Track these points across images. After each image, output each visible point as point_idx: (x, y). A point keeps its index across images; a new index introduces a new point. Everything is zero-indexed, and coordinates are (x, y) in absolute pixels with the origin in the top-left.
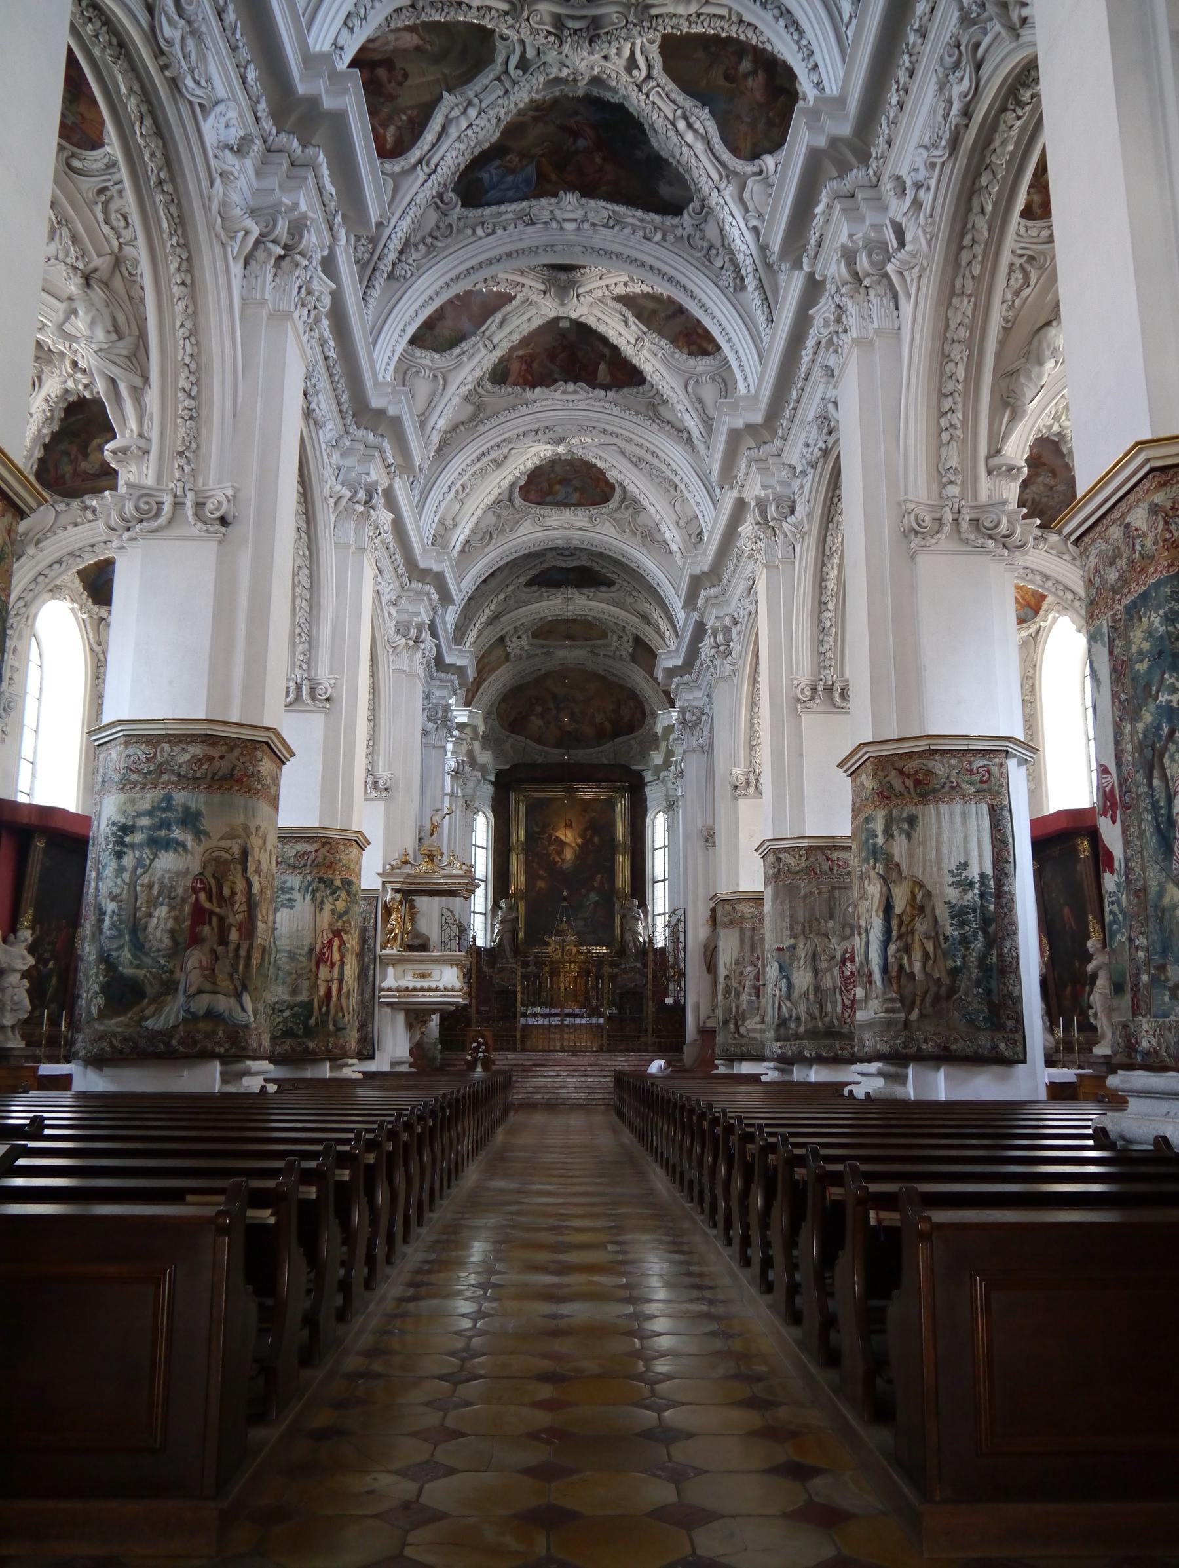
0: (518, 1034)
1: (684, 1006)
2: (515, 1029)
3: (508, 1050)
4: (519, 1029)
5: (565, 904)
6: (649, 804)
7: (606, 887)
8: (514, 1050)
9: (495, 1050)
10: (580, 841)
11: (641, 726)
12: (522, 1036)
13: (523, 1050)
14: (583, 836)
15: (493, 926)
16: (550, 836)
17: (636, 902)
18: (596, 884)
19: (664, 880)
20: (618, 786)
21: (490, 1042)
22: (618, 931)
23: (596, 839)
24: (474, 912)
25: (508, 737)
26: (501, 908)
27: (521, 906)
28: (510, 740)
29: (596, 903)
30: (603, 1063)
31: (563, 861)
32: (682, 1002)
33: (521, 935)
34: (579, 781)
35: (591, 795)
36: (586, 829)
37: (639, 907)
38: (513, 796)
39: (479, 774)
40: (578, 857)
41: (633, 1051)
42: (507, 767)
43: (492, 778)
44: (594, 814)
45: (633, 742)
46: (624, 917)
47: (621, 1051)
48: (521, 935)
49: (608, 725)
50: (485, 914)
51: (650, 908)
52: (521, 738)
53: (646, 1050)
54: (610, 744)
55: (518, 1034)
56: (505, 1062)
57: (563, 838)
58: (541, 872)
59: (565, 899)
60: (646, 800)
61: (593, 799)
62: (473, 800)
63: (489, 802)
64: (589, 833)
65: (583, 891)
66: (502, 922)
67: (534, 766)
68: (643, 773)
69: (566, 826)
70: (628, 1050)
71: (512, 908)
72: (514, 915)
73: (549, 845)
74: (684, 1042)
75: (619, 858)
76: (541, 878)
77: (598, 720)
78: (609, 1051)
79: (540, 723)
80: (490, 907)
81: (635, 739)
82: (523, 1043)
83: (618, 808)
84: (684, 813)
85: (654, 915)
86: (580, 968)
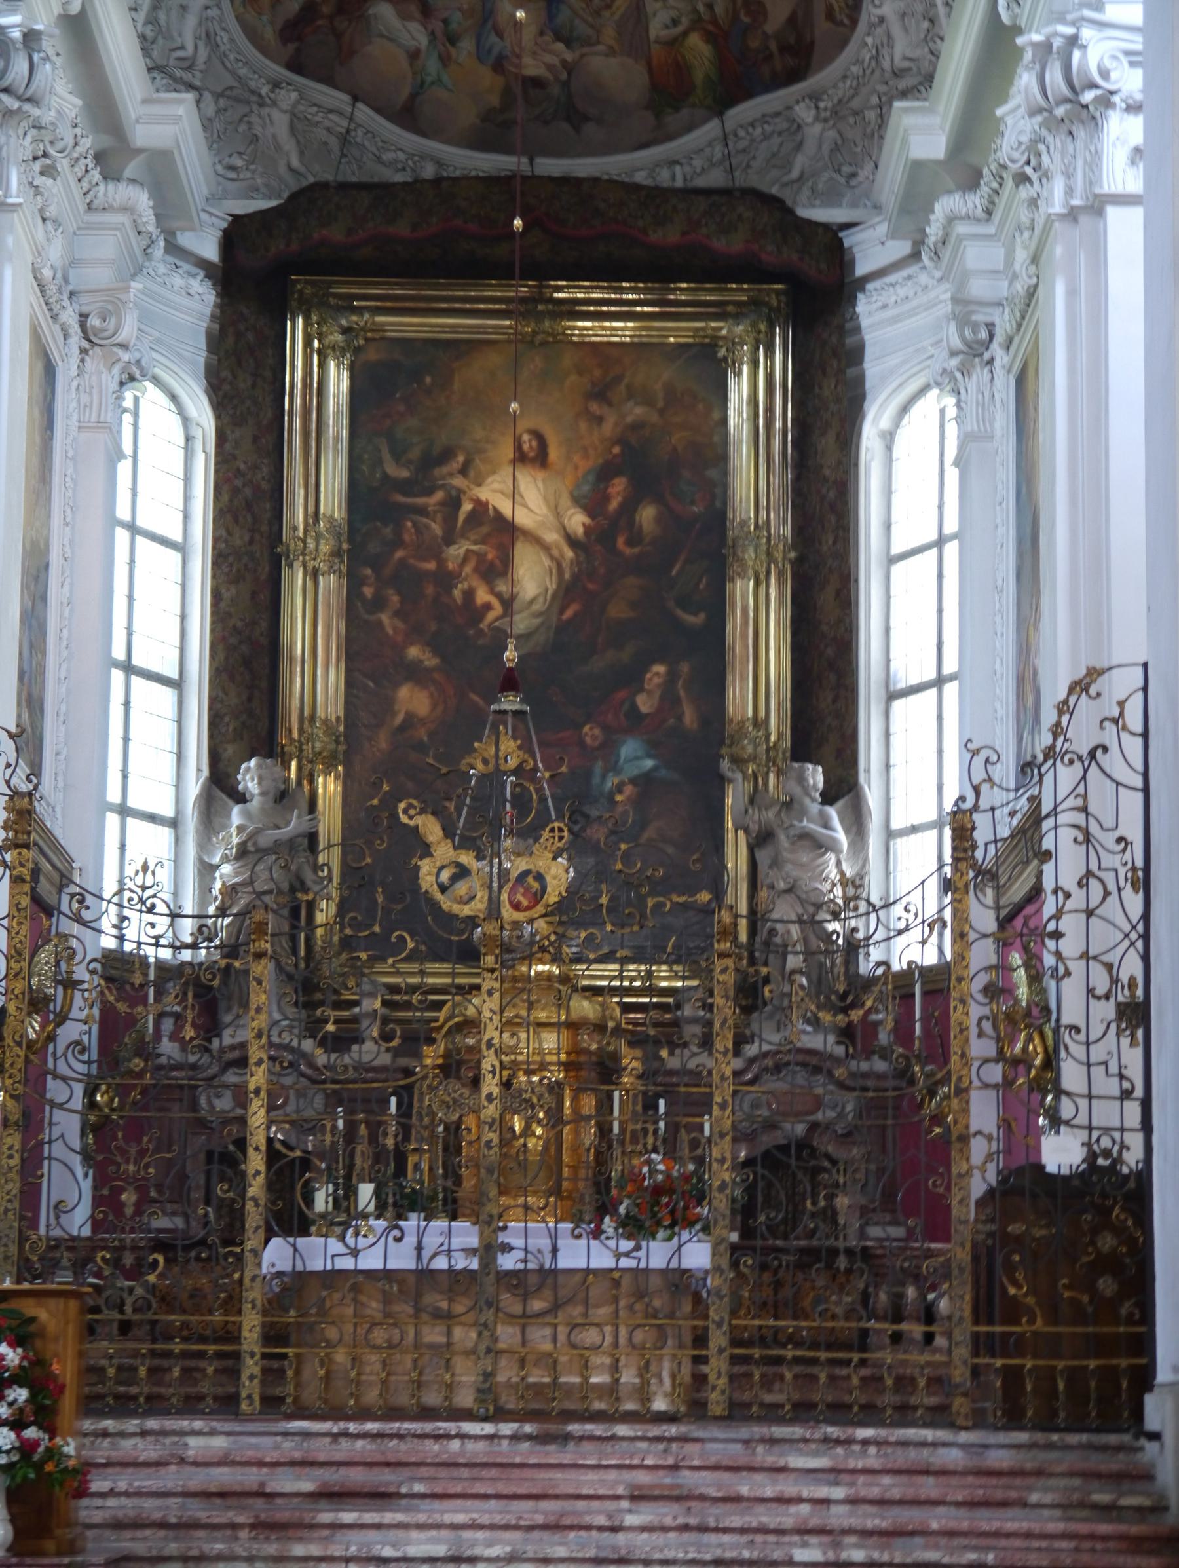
0: (251, 1325)
1: (1144, 1177)
2: (233, 1304)
3: (191, 1405)
4: (254, 1294)
5: (510, 703)
6: (872, 367)
7: (689, 717)
8: (228, 1405)
9: (92, 1405)
10: (577, 521)
11: (844, 43)
12: (274, 1336)
13: (272, 1405)
14: (592, 505)
15: (206, 870)
16: (453, 503)
17: (816, 776)
18: (645, 704)
19: (939, 681)
20: (738, 292)
21: (64, 1368)
22: (739, 897)
23: (647, 515)
24: (124, 811)
25: (276, 85)
26: (241, 798)
27: (329, 787)
28: (287, 98)
29: (645, 782)
30: (705, 1482)
31: (508, 603)
32: (1133, 1158)
33: (325, 912)
34: (574, 273)
35: (622, 331)
36: (605, 473)
37: (828, 798)
38: (297, 329)
39: (143, 200)
40: (567, 591)
41: (870, 1414)
42: (274, 203)
43: (211, 251)
44: (636, 412)
45: (804, 112)
46: (761, 839)
47: (803, 1411)
48: (325, 912)
49: (698, 48)
50: (174, 823)
51: (872, 798)
52: (339, 98)
53: (940, 1416)
54: (711, 129)
55: (251, 1325)
56: (170, 1478)
57: (505, 508)
58: (413, 652)
59: (510, 682)
60: (856, 355)
61: (637, 348)
62: (113, 309)
63: (198, 352)
64: (618, 487)
65: (591, 733)
66: (242, 852)
67: (381, 191)
68: (849, 239)
69: (521, 458)
70: (839, 1412)
71: (282, 797)
72: (295, 824)
73: (449, 540)
74: (1144, 1379)
75: (742, 590)
76: (415, 674)
77: (656, 28)
78: (737, 1413)
79: (416, 34)
80: (193, 788)
81: (815, 97)
82: (272, 1373)
83: (739, 390)
84: (1072, 293)
85: (890, 835)
86: (576, 1050)
